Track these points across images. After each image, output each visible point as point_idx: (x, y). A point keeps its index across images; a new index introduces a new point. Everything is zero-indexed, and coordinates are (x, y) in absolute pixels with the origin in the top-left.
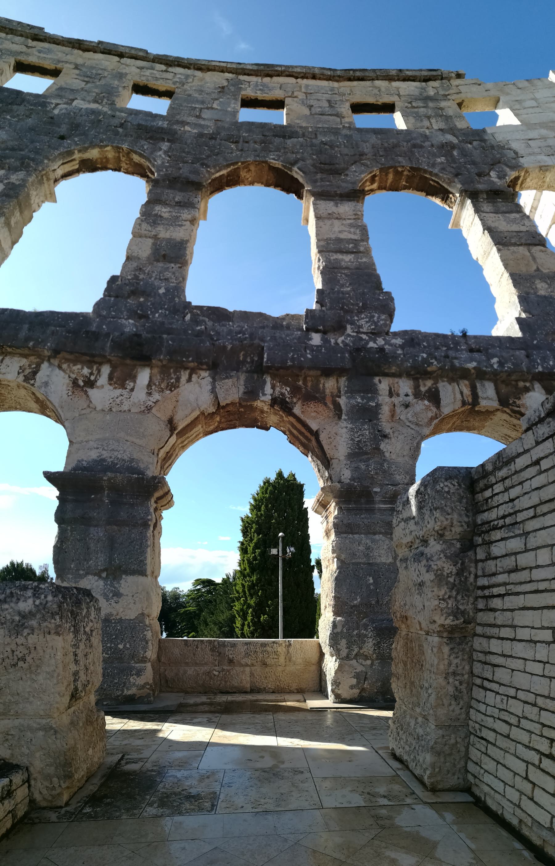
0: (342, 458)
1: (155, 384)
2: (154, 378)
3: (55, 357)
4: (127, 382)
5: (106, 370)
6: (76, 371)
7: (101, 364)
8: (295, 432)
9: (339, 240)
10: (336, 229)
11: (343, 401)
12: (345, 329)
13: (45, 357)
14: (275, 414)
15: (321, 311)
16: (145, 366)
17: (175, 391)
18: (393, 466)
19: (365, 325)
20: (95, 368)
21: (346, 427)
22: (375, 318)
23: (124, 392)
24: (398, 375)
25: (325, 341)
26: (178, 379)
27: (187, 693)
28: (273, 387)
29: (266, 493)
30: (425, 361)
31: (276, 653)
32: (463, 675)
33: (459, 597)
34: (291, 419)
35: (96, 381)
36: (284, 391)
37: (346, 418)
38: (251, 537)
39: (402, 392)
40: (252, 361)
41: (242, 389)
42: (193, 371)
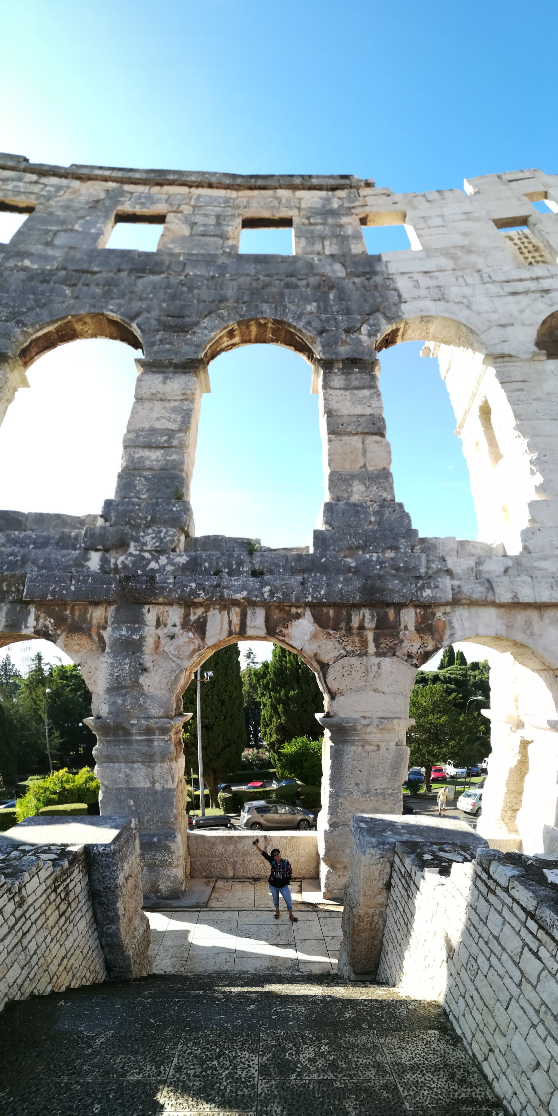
0: (101, 693)
9: (153, 431)
10: (155, 415)
11: (106, 634)
12: (128, 546)
19: (150, 541)
25: (104, 561)
36: (47, 623)
39: (170, 623)
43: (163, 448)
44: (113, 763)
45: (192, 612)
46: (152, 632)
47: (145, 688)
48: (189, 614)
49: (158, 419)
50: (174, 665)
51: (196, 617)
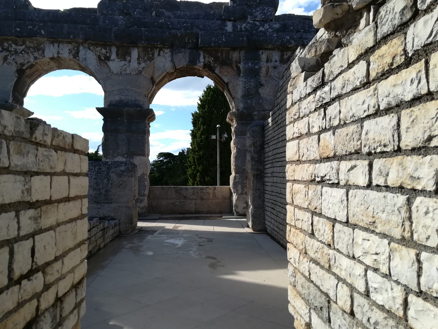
0: (239, 97)
1: (141, 58)
2: (140, 54)
3: (85, 43)
4: (127, 57)
5: (114, 50)
6: (99, 51)
7: (110, 46)
8: (217, 81)
11: (241, 66)
12: (247, 18)
13: (80, 42)
14: (206, 72)
15: (233, 7)
16: (134, 47)
17: (152, 62)
18: (264, 101)
19: (259, 16)
20: (108, 49)
21: (242, 81)
22: (266, 11)
23: (126, 63)
24: (273, 49)
25: (234, 27)
26: (153, 55)
27: (162, 213)
28: (204, 58)
29: (209, 96)
30: (288, 41)
31: (208, 193)
32: (261, 190)
33: (259, 165)
34: (214, 75)
35: (110, 56)
36: (210, 60)
37: (243, 75)
38: (198, 127)
39: (273, 60)
40: (193, 41)
41: (187, 59)
42: (160, 49)
44: (244, 136)
45: (285, 54)
46: (265, 65)
47: (262, 95)
48: (283, 55)
50: (276, 82)
51: (287, 56)
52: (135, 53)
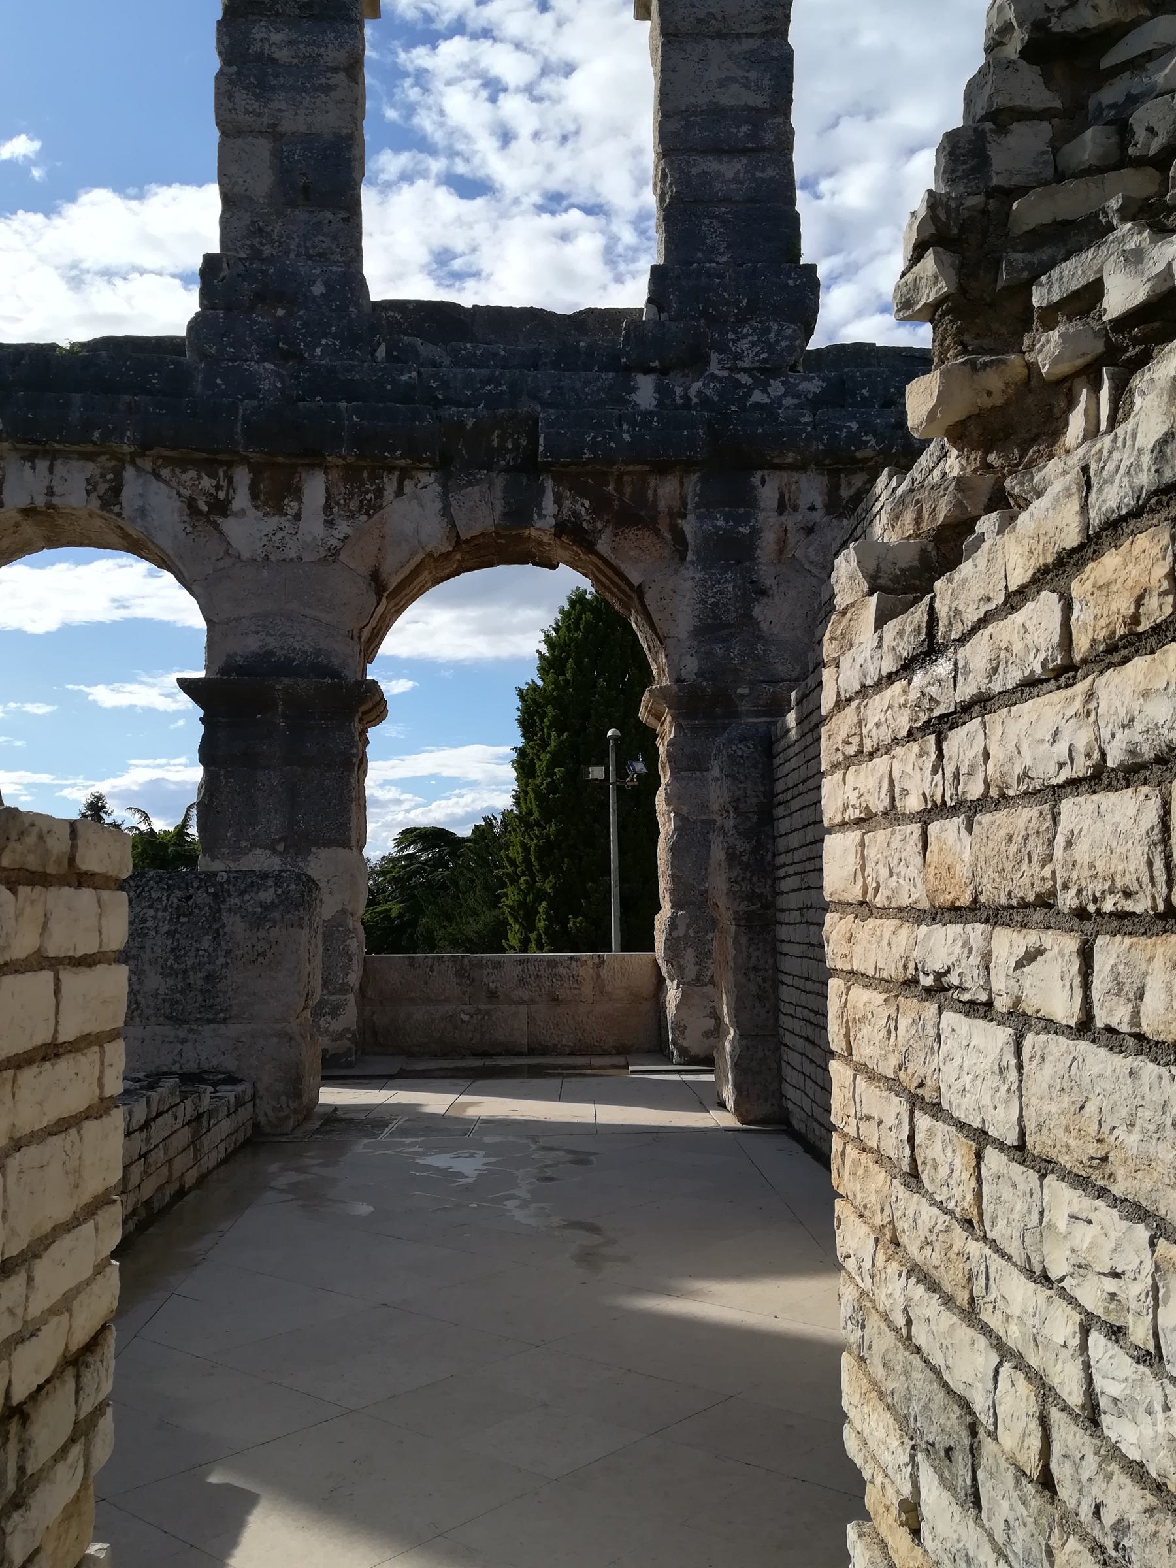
0: (683, 635)
1: (338, 504)
2: (334, 491)
3: (143, 455)
4: (286, 501)
5: (242, 477)
6: (189, 483)
7: (230, 465)
8: (604, 580)
11: (689, 526)
12: (707, 362)
13: (124, 454)
14: (564, 548)
15: (659, 324)
16: (312, 466)
17: (376, 517)
18: (773, 649)
19: (748, 349)
20: (221, 474)
21: (693, 578)
22: (772, 335)
23: (285, 522)
24: (801, 467)
25: (663, 392)
26: (379, 492)
27: (410, 1055)
28: (558, 501)
29: (577, 629)
30: (854, 438)
31: (575, 978)
32: (766, 970)
33: (755, 879)
34: (594, 559)
35: (229, 501)
36: (578, 507)
37: (695, 558)
38: (542, 738)
39: (803, 503)
40: (517, 446)
41: (499, 507)
42: (405, 474)
43: (744, 152)
44: (701, 770)
45: (843, 482)
46: (772, 520)
47: (764, 626)
49: (723, 83)
51: (853, 491)
52: (315, 488)
